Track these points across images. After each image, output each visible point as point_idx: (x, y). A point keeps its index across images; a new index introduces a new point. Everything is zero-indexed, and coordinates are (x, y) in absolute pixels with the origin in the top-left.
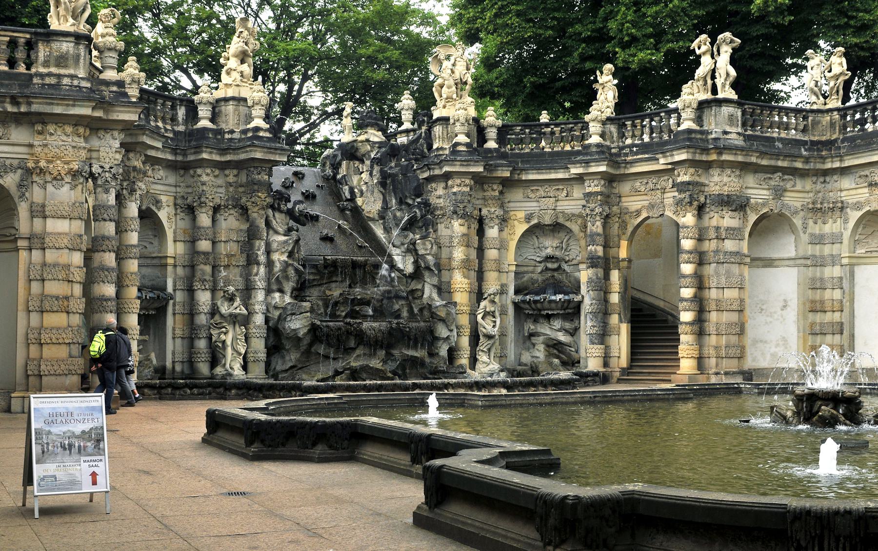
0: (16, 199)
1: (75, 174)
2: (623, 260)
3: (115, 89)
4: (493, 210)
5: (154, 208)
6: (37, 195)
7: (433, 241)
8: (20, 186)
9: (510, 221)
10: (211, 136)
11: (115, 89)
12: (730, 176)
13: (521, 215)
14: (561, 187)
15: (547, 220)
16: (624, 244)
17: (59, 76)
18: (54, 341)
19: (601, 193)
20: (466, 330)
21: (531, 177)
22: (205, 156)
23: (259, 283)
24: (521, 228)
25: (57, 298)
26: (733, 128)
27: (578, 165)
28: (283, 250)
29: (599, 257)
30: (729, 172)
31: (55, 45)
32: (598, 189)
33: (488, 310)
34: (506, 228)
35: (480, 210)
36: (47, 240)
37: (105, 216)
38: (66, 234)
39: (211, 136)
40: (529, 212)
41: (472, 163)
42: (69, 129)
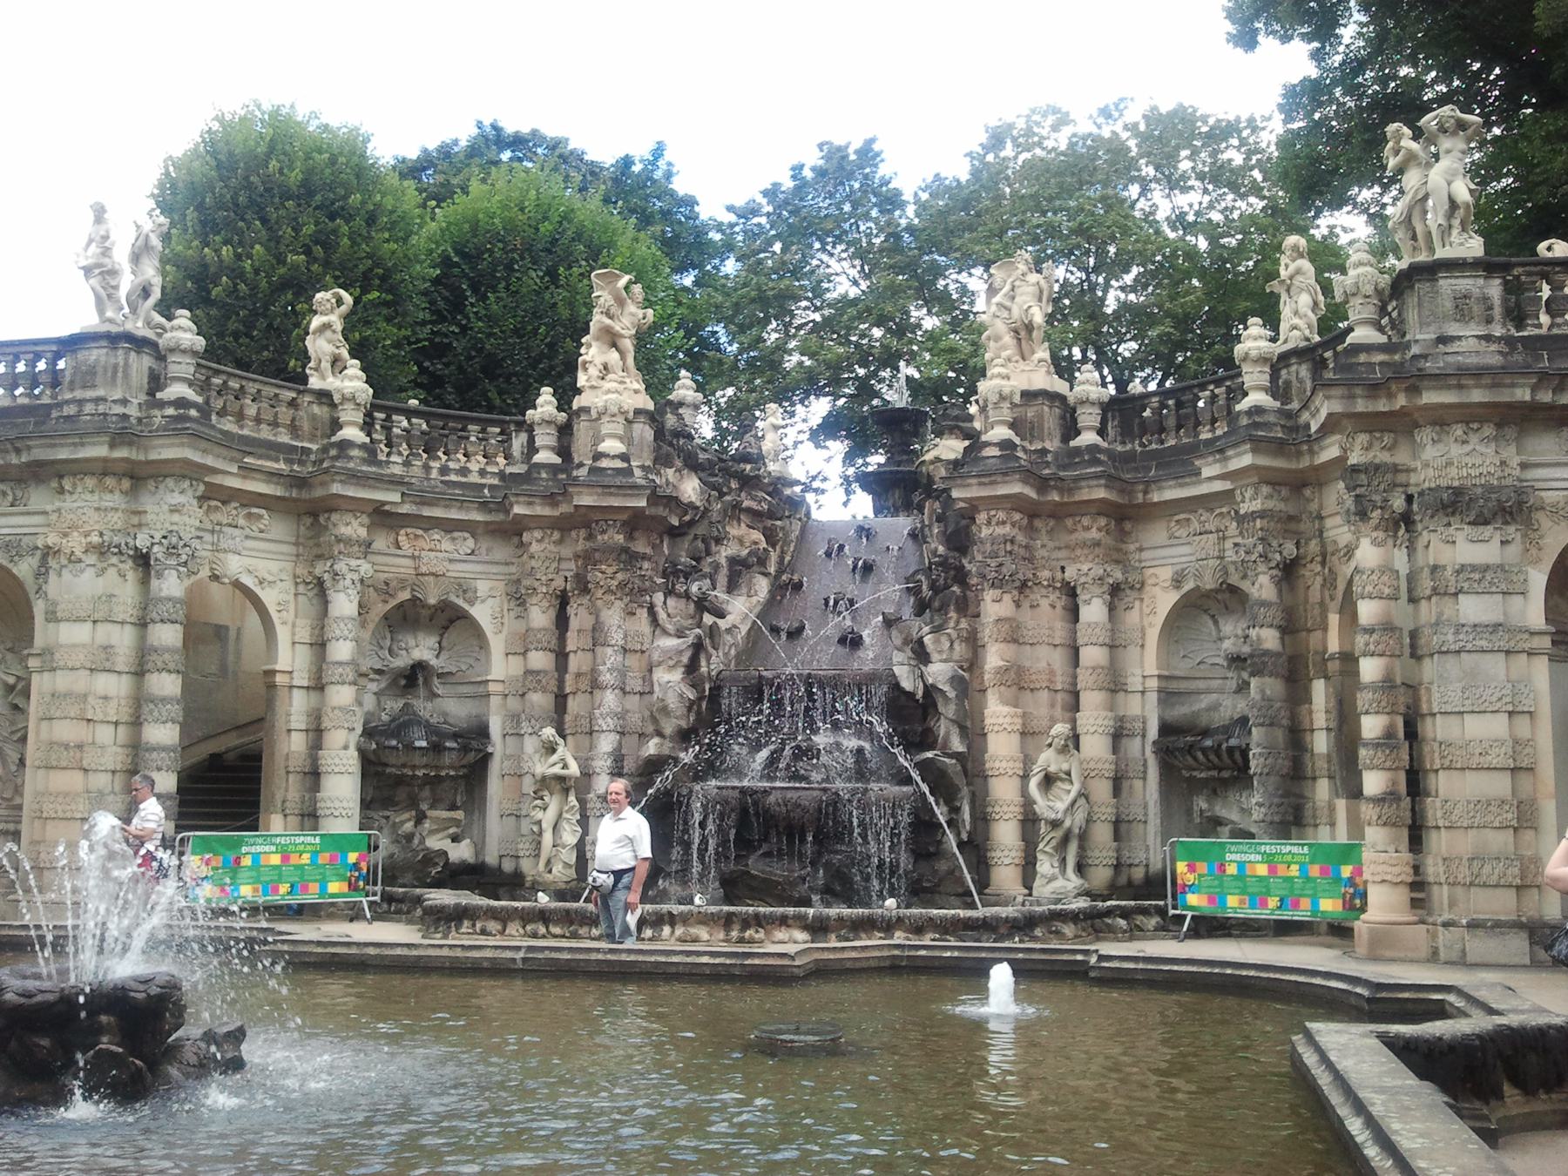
0: (32, 596)
1: (102, 550)
2: (1332, 658)
3: (170, 411)
4: (1085, 568)
5: (460, 602)
6: (53, 586)
7: (954, 635)
8: (38, 575)
9: (1147, 588)
10: (544, 475)
11: (170, 411)
12: (1464, 442)
13: (1166, 574)
14: (1224, 510)
15: (1209, 583)
16: (1334, 619)
17: (80, 402)
18: (60, 814)
19: (1262, 514)
20: (1005, 808)
21: (1171, 493)
22: (518, 510)
23: (600, 721)
24: (1164, 600)
25: (67, 747)
26: (1472, 325)
27: (1211, 459)
28: (671, 663)
29: (1266, 653)
30: (1459, 432)
31: (81, 355)
32: (1256, 505)
33: (1052, 769)
34: (1137, 603)
35: (1063, 569)
36: (57, 656)
37: (154, 615)
38: (84, 646)
39: (544, 475)
40: (1179, 567)
41: (999, 479)
42: (90, 482)
